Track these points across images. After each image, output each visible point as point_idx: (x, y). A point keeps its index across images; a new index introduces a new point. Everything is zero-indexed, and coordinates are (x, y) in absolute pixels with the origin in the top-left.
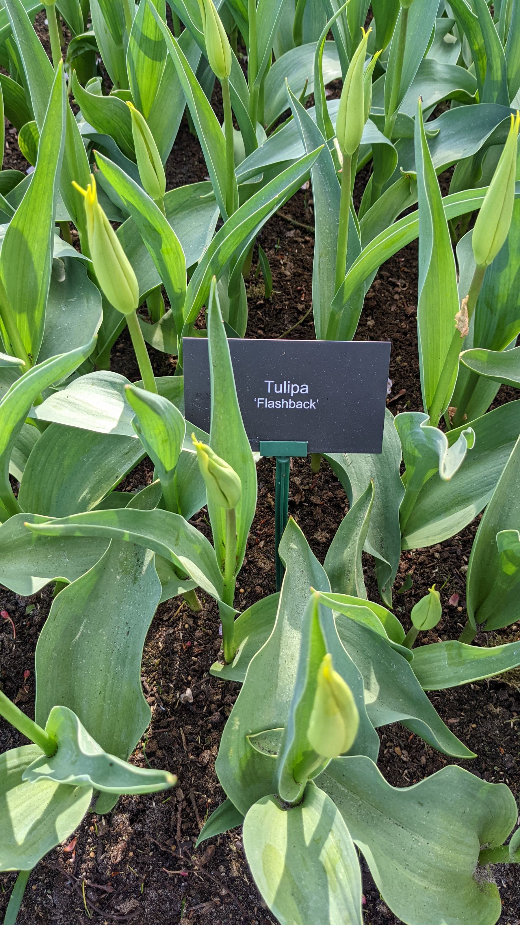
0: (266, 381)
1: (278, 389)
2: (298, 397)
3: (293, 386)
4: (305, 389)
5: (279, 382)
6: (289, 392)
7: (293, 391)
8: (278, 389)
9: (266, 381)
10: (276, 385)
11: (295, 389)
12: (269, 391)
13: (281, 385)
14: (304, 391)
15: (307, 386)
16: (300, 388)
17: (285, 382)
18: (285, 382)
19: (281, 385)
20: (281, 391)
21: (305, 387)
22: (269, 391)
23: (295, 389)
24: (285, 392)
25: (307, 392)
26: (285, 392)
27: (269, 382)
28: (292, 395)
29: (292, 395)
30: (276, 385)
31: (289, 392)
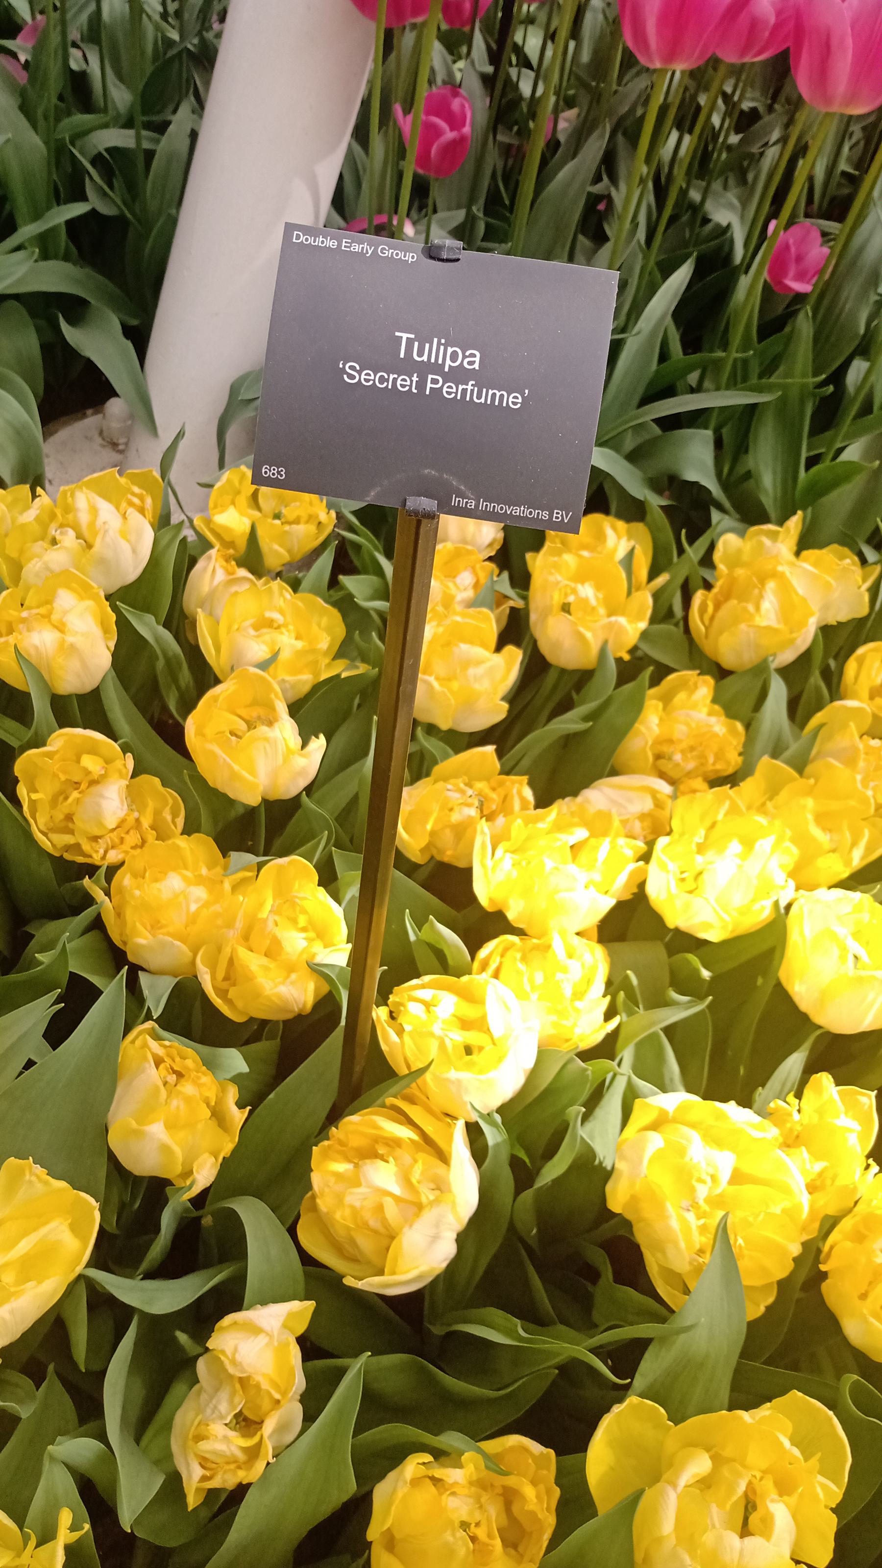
0: (397, 334)
1: (420, 353)
3: (450, 350)
4: (474, 360)
5: (424, 339)
6: (440, 362)
7: (448, 362)
8: (420, 353)
9: (397, 334)
10: (416, 344)
12: (402, 356)
13: (427, 346)
14: (470, 363)
15: (478, 354)
16: (464, 357)
17: (436, 340)
18: (436, 340)
19: (427, 346)
20: (425, 358)
21: (474, 356)
22: (402, 356)
24: (433, 360)
25: (476, 366)
26: (433, 360)
27: (405, 336)
28: (446, 369)
29: (446, 369)
30: (416, 344)
31: (440, 362)
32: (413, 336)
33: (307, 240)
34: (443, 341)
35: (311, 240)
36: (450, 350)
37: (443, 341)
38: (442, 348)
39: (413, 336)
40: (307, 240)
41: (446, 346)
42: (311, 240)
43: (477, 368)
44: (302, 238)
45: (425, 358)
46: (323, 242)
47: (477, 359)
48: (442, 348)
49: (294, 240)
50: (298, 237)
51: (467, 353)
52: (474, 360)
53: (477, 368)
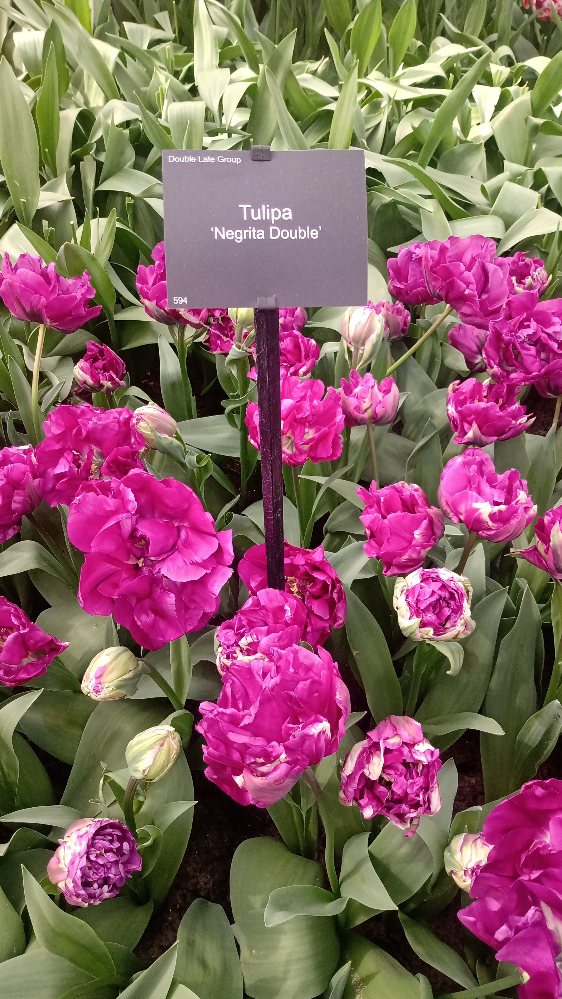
0: (240, 206)
1: (256, 215)
2: (282, 224)
4: (288, 214)
5: (256, 206)
6: (268, 218)
7: (273, 218)
8: (256, 215)
9: (240, 206)
10: (252, 210)
11: (276, 214)
12: (245, 218)
14: (286, 216)
16: (282, 213)
17: (264, 206)
18: (264, 206)
19: (259, 210)
22: (245, 218)
23: (276, 214)
24: (264, 218)
25: (290, 217)
26: (264, 218)
27: (245, 207)
28: (273, 222)
29: (273, 222)
30: (252, 210)
31: (268, 218)
32: (249, 206)
33: (177, 160)
34: (268, 206)
35: (180, 159)
36: (273, 210)
37: (268, 206)
38: (268, 210)
39: (249, 206)
40: (177, 160)
41: (270, 208)
42: (180, 159)
43: (291, 219)
44: (175, 159)
45: (259, 218)
46: (187, 160)
47: (290, 213)
48: (268, 210)
49: (170, 161)
50: (172, 159)
51: (284, 211)
52: (288, 214)
53: (291, 219)
